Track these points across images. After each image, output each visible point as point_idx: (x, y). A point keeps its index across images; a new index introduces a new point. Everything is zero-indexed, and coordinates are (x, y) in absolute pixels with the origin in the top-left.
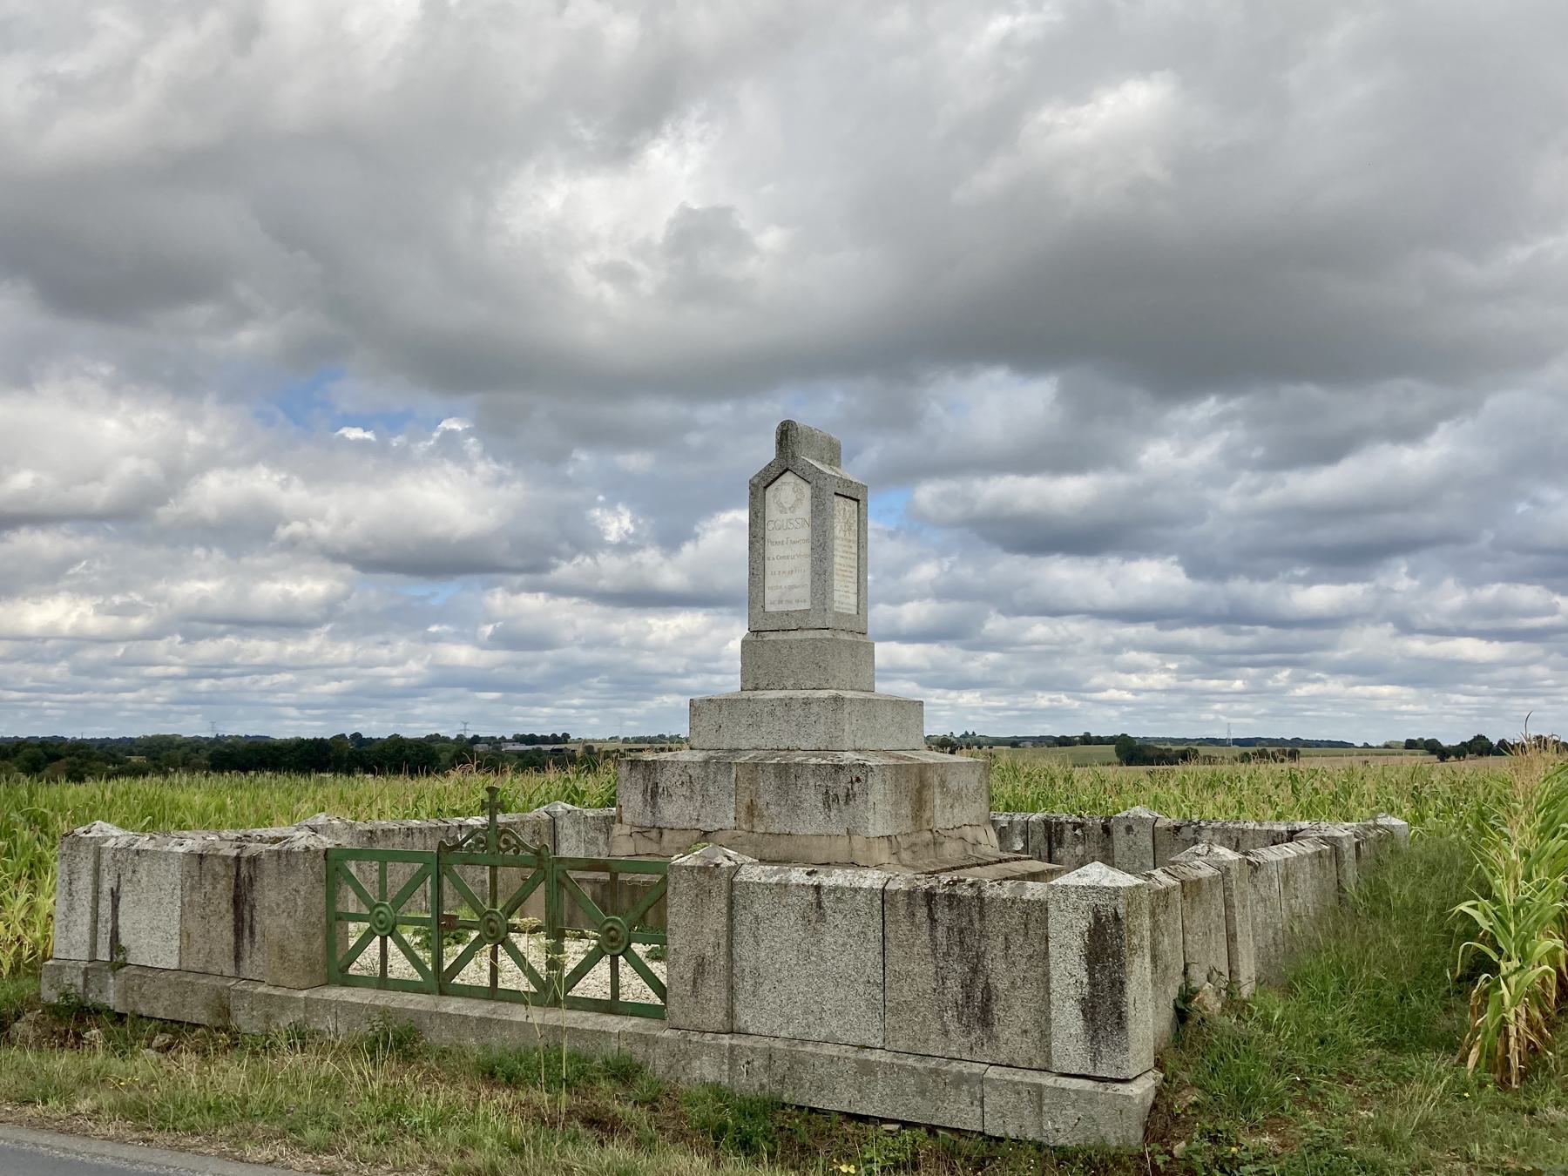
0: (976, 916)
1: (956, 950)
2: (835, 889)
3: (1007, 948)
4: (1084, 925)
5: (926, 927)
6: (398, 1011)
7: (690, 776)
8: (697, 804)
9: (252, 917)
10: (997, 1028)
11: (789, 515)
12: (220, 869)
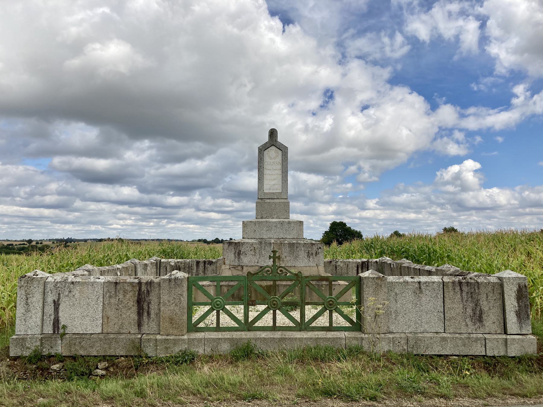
0: (476, 288)
1: (470, 299)
2: (426, 283)
3: (487, 297)
4: (515, 289)
5: (459, 293)
9: (149, 307)
10: (484, 322)
12: (129, 288)
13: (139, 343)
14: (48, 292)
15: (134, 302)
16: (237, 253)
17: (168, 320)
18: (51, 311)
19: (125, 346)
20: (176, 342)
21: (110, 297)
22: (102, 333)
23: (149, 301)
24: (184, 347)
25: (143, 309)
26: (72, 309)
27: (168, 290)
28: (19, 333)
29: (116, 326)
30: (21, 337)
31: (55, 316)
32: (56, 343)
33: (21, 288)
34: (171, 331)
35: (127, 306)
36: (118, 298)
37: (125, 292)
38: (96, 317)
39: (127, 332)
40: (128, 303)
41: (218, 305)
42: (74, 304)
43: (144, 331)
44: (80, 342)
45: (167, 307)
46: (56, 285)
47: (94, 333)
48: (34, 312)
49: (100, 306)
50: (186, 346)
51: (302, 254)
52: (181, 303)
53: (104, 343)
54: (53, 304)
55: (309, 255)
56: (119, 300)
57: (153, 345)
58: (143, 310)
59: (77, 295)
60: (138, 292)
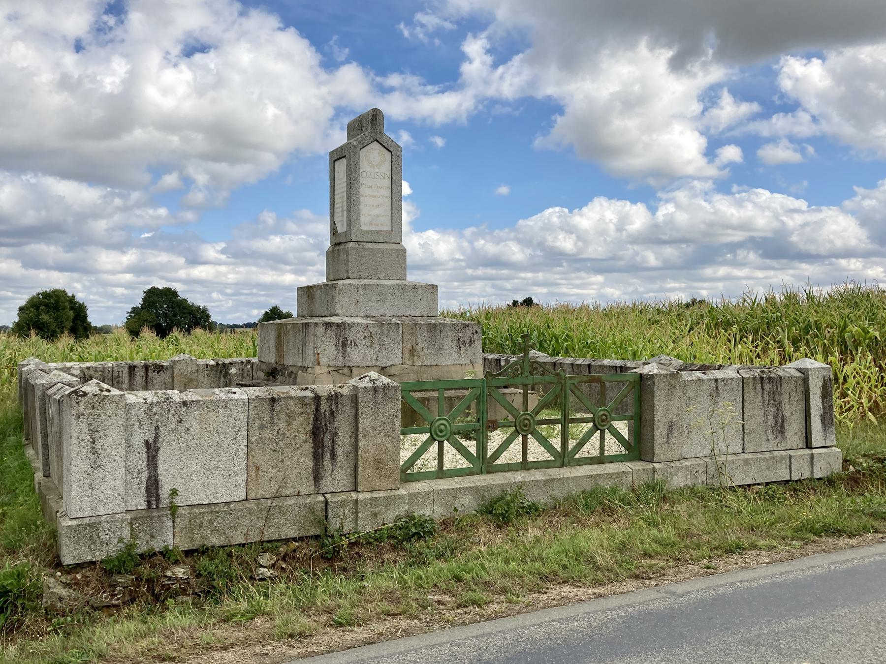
0: (779, 386)
1: (772, 401)
2: (723, 380)
3: (790, 398)
4: (820, 384)
5: (760, 394)
6: (488, 488)
7: (371, 333)
8: (376, 350)
9: (333, 443)
10: (786, 434)
11: (376, 170)
12: (297, 408)
13: (322, 510)
14: (133, 425)
15: (307, 434)
16: (340, 342)
17: (372, 463)
18: (140, 462)
19: (297, 520)
20: (389, 503)
21: (262, 427)
22: (246, 500)
23: (334, 431)
24: (402, 509)
25: (323, 447)
26: (184, 458)
27: (372, 408)
28: (79, 515)
29: (272, 483)
30: (86, 521)
31: (150, 473)
32: (162, 528)
33: (79, 418)
34: (377, 483)
35: (293, 442)
36: (276, 428)
37: (290, 416)
38: (235, 469)
39: (293, 494)
40: (295, 436)
41: (441, 431)
42: (189, 447)
43: (325, 489)
44: (211, 520)
45: (370, 439)
46: (150, 410)
47: (231, 500)
48: (109, 467)
49: (242, 447)
50: (406, 508)
51: (449, 343)
52: (394, 430)
53: (258, 518)
54: (145, 450)
55: (460, 344)
56: (278, 432)
57: (349, 511)
58: (323, 449)
59: (195, 428)
60: (315, 415)
